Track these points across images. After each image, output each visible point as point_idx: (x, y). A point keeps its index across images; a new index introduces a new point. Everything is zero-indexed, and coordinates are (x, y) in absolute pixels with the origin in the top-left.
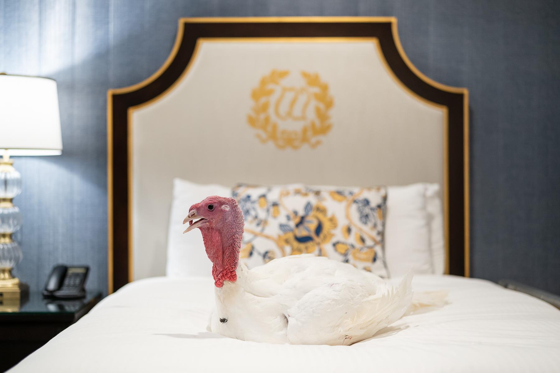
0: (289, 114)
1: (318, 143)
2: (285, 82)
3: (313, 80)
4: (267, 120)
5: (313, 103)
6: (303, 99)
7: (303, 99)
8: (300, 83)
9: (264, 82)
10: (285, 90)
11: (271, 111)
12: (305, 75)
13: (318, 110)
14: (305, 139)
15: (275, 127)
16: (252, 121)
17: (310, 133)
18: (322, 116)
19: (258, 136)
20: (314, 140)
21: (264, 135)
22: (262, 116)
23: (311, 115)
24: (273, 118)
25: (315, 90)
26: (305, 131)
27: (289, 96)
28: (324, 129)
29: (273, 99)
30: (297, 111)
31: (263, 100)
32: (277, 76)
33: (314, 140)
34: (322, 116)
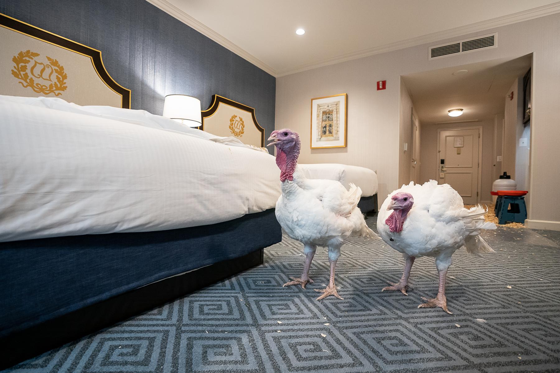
2: (36, 59)
6: (48, 71)
9: (21, 54)
10: (36, 62)
11: (28, 71)
12: (49, 59)
13: (58, 78)
15: (32, 80)
17: (54, 88)
19: (20, 82)
21: (25, 84)
22: (22, 73)
24: (30, 76)
25: (57, 68)
26: (51, 86)
30: (46, 75)
31: (23, 64)
33: (57, 92)
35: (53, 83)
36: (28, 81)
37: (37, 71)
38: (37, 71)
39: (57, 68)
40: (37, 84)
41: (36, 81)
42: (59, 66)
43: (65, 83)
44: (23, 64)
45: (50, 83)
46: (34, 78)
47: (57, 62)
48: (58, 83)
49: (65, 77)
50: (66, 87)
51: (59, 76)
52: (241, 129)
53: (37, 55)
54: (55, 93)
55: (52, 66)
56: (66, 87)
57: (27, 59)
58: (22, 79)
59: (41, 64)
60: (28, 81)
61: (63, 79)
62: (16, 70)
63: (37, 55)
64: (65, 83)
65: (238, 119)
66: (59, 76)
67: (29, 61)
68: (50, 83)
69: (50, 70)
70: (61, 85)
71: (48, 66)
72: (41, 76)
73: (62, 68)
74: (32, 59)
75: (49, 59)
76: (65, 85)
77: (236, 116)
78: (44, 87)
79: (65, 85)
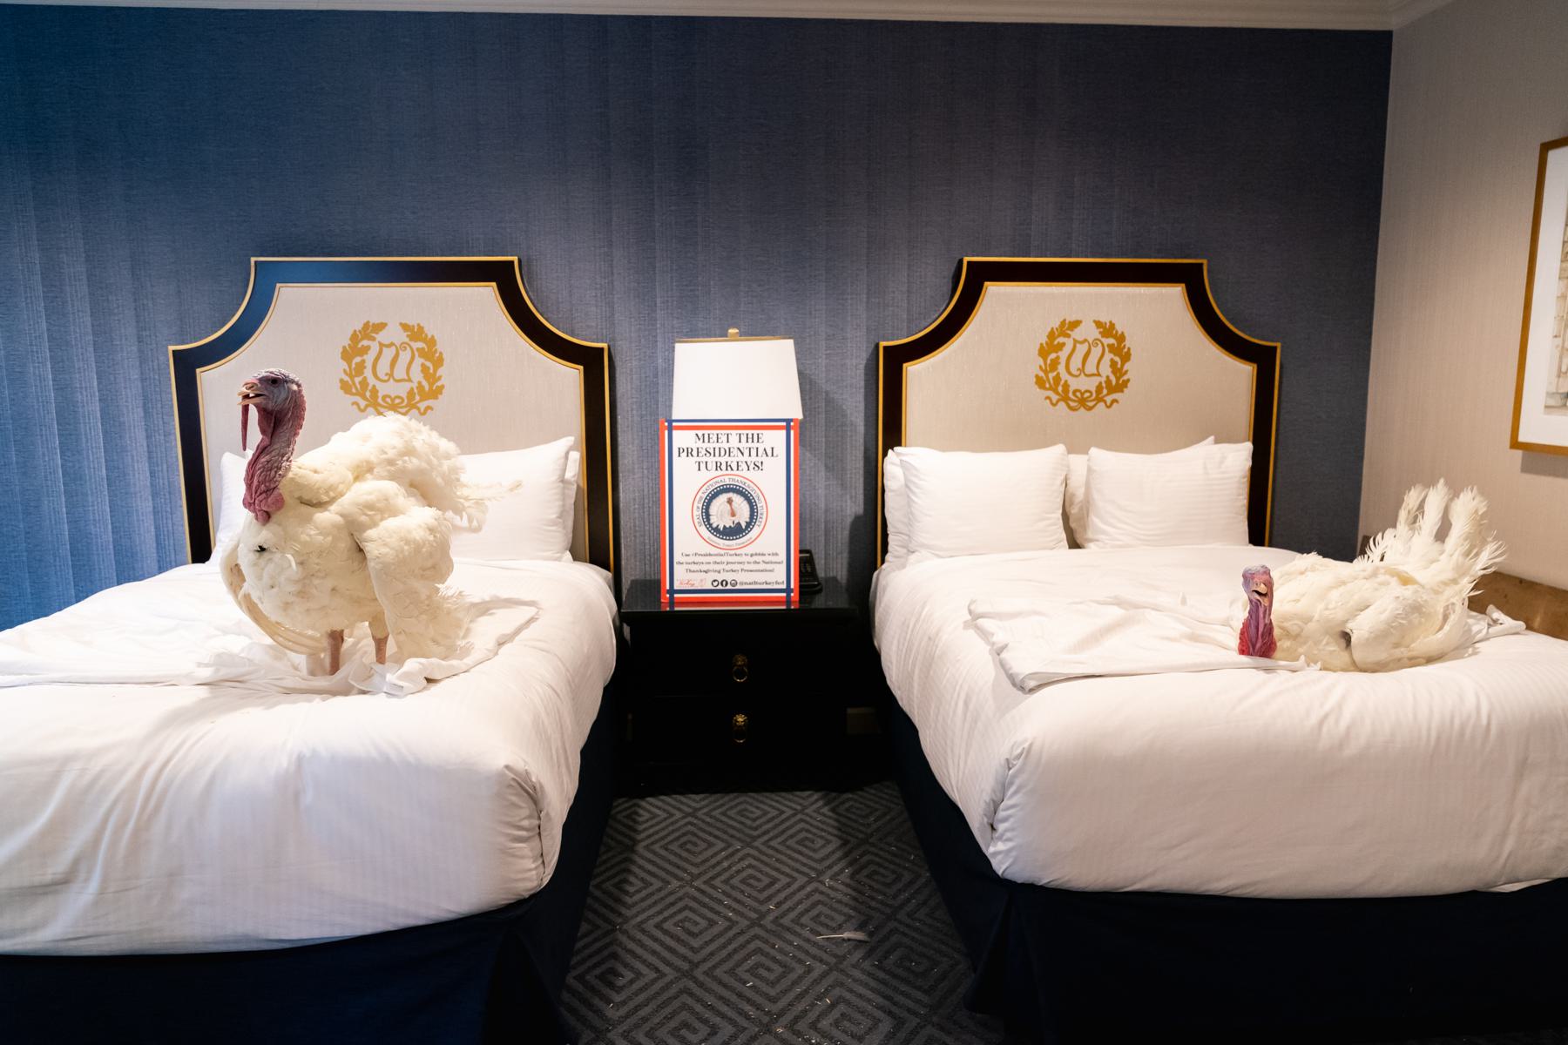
0: (391, 375)
1: (428, 408)
2: (382, 337)
3: (415, 333)
4: (364, 383)
5: (419, 361)
6: (405, 356)
7: (405, 356)
8: (402, 337)
9: (355, 338)
11: (368, 373)
12: (405, 327)
13: (424, 369)
15: (374, 391)
16: (346, 387)
18: (430, 376)
21: (363, 403)
22: (357, 380)
23: (416, 374)
24: (372, 381)
25: (420, 345)
26: (411, 393)
27: (388, 354)
29: (369, 358)
30: (400, 372)
31: (358, 359)
32: (371, 329)
34: (430, 376)
35: (415, 385)
36: (368, 394)
37: (383, 367)
38: (383, 367)
40: (385, 397)
41: (383, 389)
42: (424, 340)
44: (358, 359)
45: (406, 387)
46: (379, 386)
47: (421, 328)
48: (426, 384)
49: (439, 362)
51: (428, 364)
52: (1106, 370)
53: (382, 326)
57: (365, 343)
58: (357, 394)
59: (392, 344)
60: (368, 394)
62: (347, 378)
63: (382, 326)
65: (1088, 331)
66: (428, 364)
67: (368, 348)
70: (431, 385)
71: (404, 346)
72: (391, 375)
73: (432, 342)
74: (374, 339)
75: (405, 327)
77: (1075, 324)
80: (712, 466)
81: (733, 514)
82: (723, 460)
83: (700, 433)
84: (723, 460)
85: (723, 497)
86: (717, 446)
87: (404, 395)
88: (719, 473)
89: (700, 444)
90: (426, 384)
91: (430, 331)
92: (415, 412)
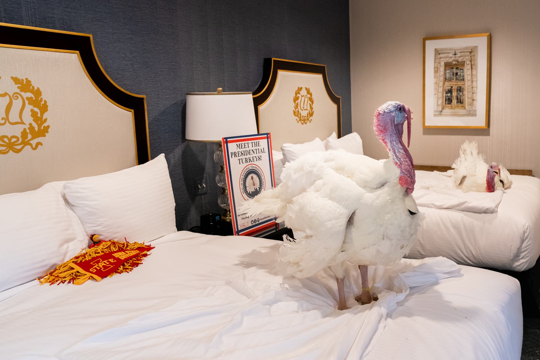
3: (25, 85)
5: (29, 107)
6: (17, 104)
7: (17, 104)
8: (14, 88)
12: (16, 80)
13: (34, 114)
14: (25, 143)
17: (30, 137)
18: (39, 119)
20: (34, 142)
23: (28, 118)
25: (29, 95)
26: (24, 134)
28: (43, 132)
30: (14, 116)
33: (34, 142)
34: (39, 119)
35: (27, 127)
39: (29, 95)
42: (32, 91)
43: (46, 120)
45: (21, 128)
47: (29, 82)
48: (35, 125)
49: (44, 108)
50: (48, 127)
51: (36, 109)
54: (31, 145)
55: (22, 94)
56: (48, 127)
59: (6, 94)
61: (42, 115)
64: (46, 120)
66: (36, 109)
68: (21, 128)
69: (20, 101)
70: (39, 126)
71: (16, 96)
73: (38, 93)
75: (16, 80)
76: (46, 125)
78: (13, 140)
79: (46, 125)
80: (244, 161)
81: (254, 185)
82: (247, 157)
83: (238, 143)
84: (247, 157)
85: (250, 177)
86: (245, 149)
87: (19, 135)
88: (247, 164)
89: (239, 150)
90: (35, 125)
91: (35, 84)
92: (28, 147)
